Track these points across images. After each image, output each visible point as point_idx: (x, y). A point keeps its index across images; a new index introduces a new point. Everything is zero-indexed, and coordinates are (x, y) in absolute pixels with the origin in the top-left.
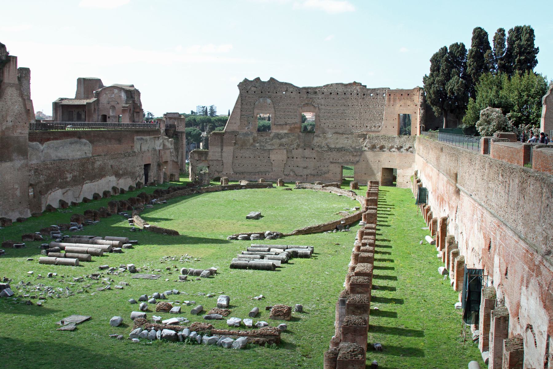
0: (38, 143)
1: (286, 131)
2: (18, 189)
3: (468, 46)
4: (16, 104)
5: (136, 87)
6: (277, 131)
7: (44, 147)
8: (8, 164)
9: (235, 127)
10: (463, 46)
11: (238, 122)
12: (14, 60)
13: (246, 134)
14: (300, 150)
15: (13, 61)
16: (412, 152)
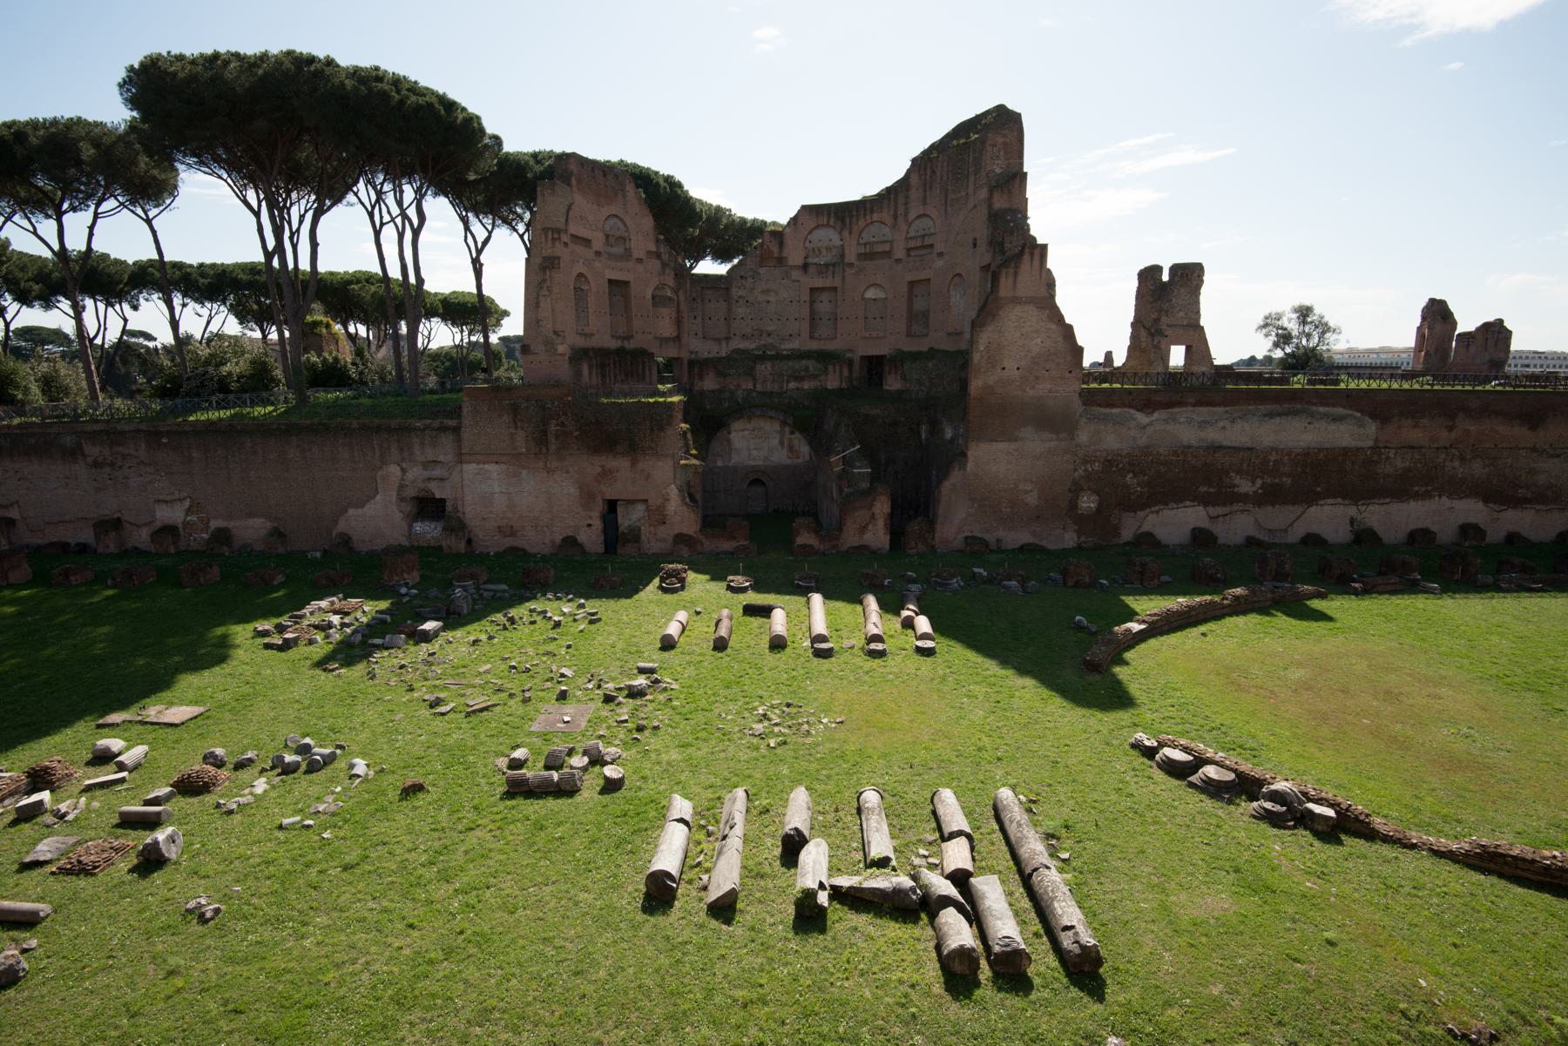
0: (1132, 411)
2: (1031, 491)
4: (1035, 335)
7: (1154, 418)
8: (1001, 446)
12: (1037, 252)
15: (1032, 255)
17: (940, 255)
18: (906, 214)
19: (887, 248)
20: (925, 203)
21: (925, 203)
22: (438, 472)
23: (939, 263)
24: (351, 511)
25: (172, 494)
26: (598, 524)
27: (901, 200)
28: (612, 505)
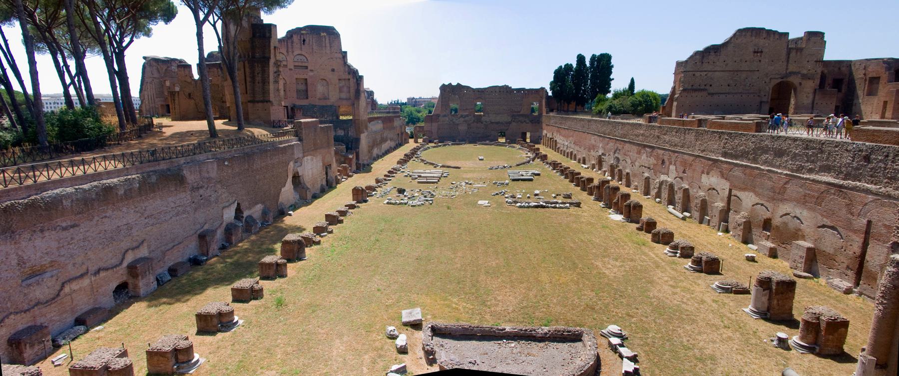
1: (467, 113)
3: (575, 66)
5: (371, 89)
6: (461, 113)
9: (438, 112)
10: (571, 65)
11: (440, 109)
13: (445, 116)
14: (475, 123)
16: (539, 123)
17: (311, 71)
18: (293, 52)
19: (285, 63)
20: (301, 49)
21: (301, 49)
22: (299, 164)
23: (311, 74)
24: (283, 190)
25: (229, 201)
26: (325, 176)
27: (289, 44)
28: (326, 168)
